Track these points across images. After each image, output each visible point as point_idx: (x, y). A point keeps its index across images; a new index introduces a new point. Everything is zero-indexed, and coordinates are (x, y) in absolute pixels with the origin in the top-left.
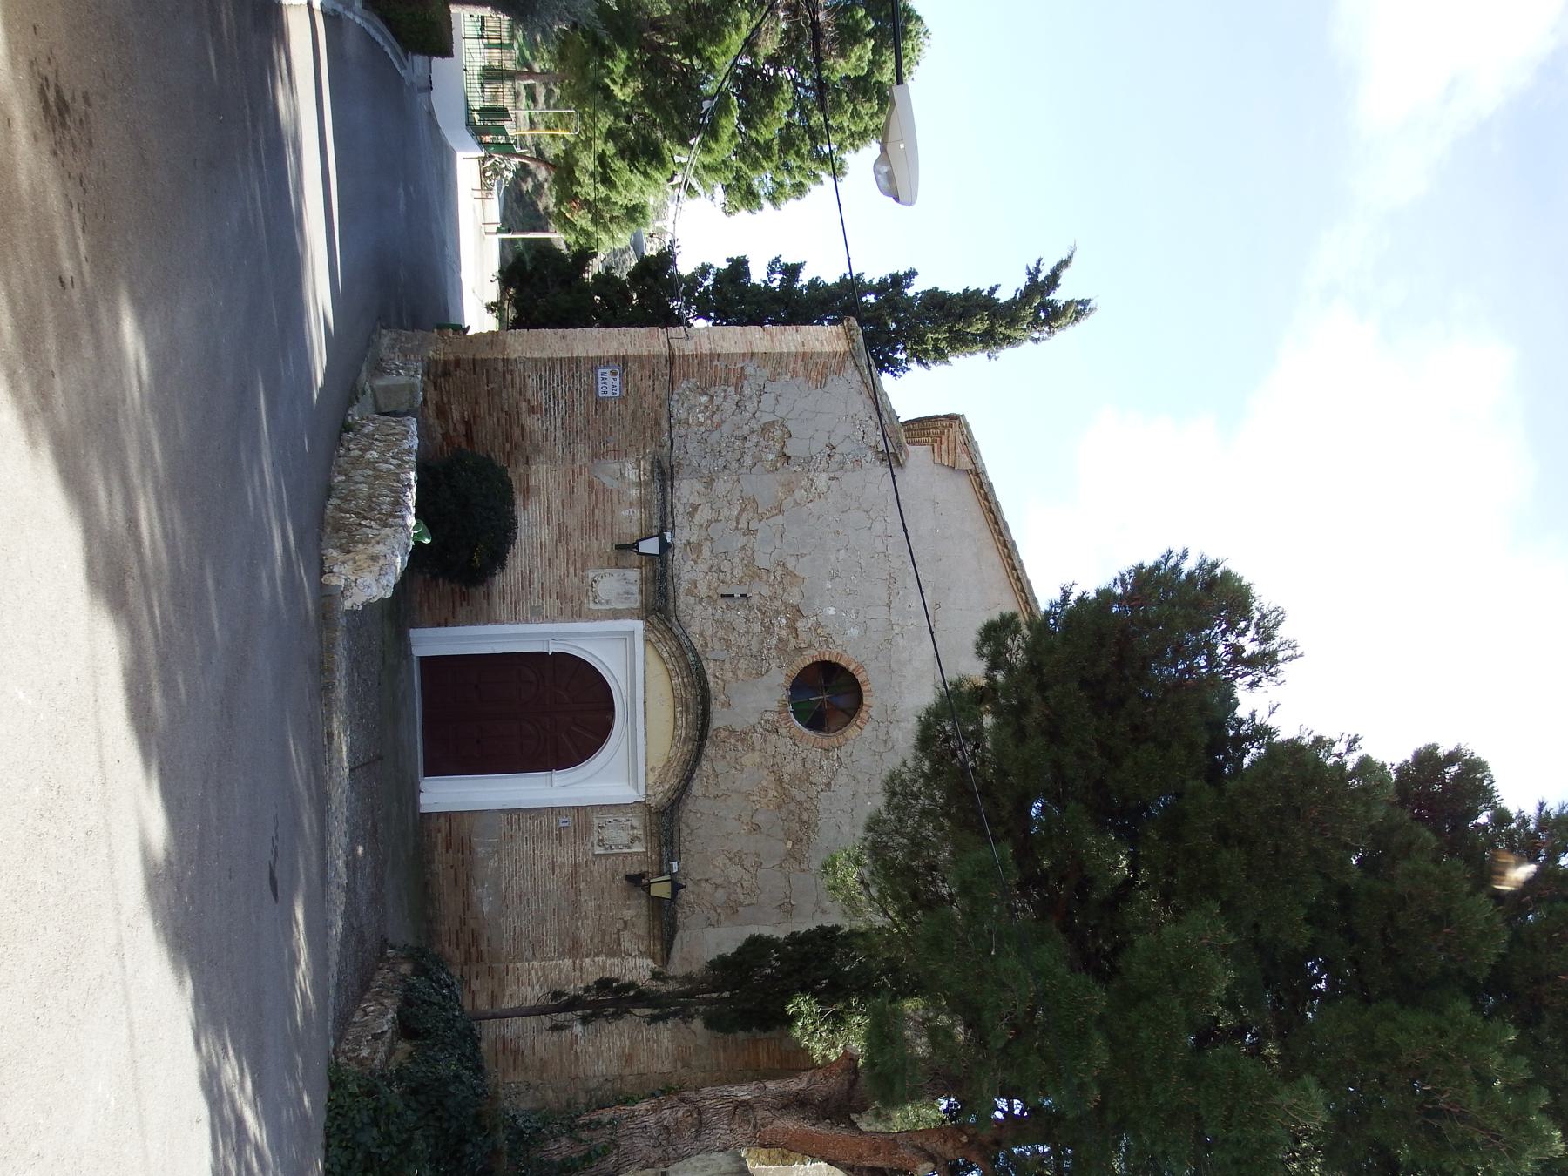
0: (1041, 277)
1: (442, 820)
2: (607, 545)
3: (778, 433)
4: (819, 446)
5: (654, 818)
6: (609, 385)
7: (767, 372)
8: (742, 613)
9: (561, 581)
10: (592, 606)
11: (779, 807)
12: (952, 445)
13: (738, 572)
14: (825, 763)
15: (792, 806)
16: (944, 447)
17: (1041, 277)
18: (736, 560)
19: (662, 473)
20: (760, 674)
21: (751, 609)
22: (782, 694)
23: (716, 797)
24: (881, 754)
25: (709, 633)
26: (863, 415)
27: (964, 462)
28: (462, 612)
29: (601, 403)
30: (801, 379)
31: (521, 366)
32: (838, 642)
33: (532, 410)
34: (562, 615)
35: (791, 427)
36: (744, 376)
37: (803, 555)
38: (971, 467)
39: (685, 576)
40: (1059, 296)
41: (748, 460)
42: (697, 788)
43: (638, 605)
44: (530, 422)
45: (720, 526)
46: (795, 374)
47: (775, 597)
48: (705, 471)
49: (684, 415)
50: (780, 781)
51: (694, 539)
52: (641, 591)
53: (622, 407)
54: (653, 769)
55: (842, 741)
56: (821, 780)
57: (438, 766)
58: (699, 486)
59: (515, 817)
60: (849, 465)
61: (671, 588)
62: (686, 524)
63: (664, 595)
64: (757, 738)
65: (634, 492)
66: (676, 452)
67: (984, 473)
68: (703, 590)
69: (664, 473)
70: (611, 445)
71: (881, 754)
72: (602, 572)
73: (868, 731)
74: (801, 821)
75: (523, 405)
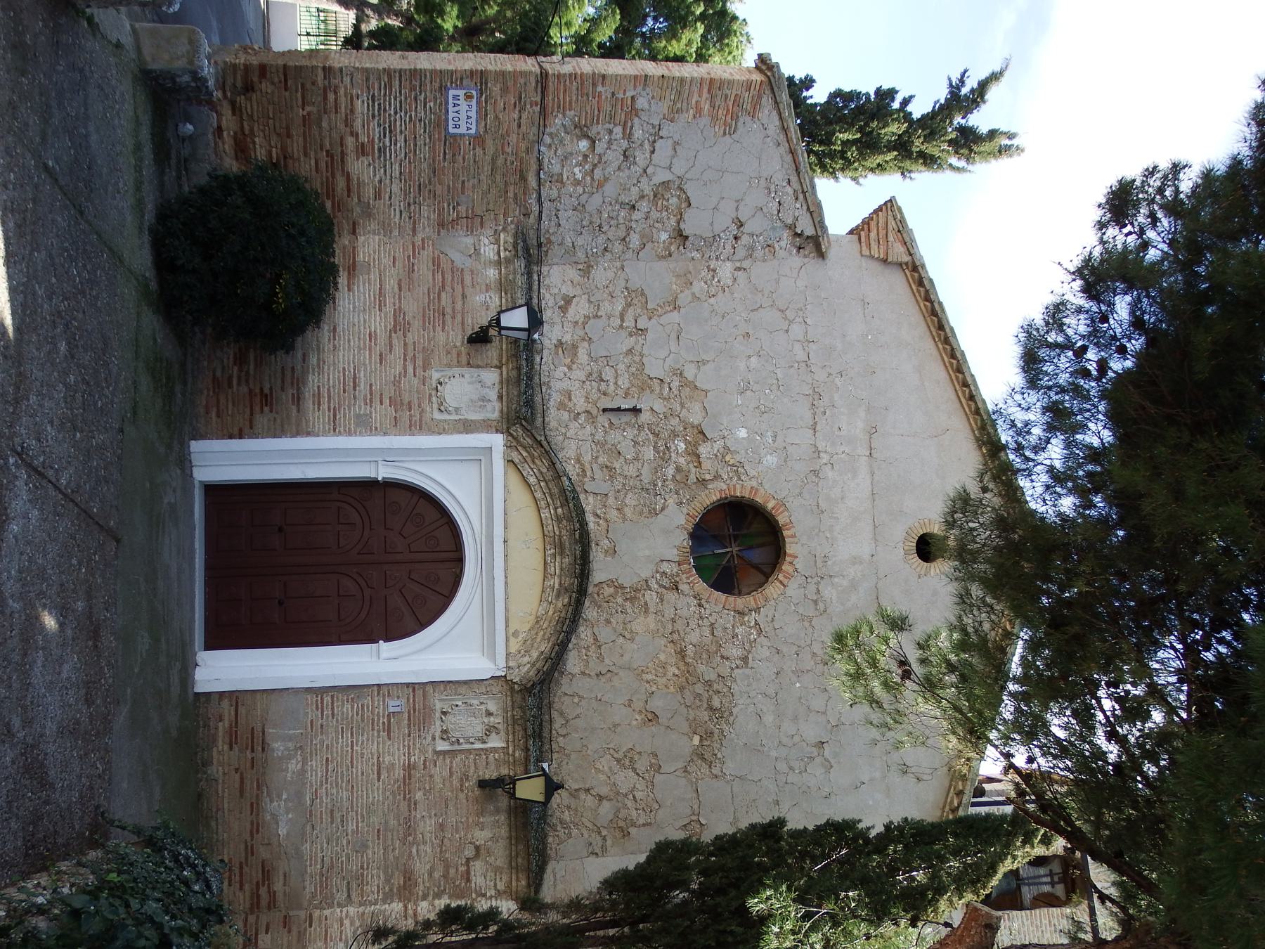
0: (964, 91)
1: (225, 703)
2: (456, 337)
3: (674, 201)
4: (723, 222)
5: (518, 698)
6: (463, 115)
7: (664, 107)
8: (630, 433)
9: (396, 383)
10: (437, 415)
11: (682, 689)
12: (882, 233)
13: (624, 382)
14: (740, 630)
15: (699, 688)
16: (873, 235)
17: (964, 91)
18: (621, 367)
19: (527, 249)
20: (654, 513)
21: (640, 428)
22: (683, 539)
23: (599, 675)
24: (810, 619)
25: (587, 458)
26: (779, 178)
27: (898, 252)
28: (261, 420)
29: (452, 142)
30: (705, 120)
31: (347, 80)
32: (752, 473)
33: (362, 150)
34: (397, 426)
35: (690, 189)
36: (634, 112)
37: (705, 362)
38: (906, 258)
39: (556, 385)
40: (980, 120)
41: (635, 240)
42: (573, 663)
43: (496, 415)
44: (360, 168)
45: (601, 323)
46: (698, 112)
47: (671, 414)
48: (581, 255)
49: (556, 168)
50: (682, 654)
51: (567, 338)
52: (500, 397)
53: (479, 151)
54: (516, 634)
55: (761, 602)
56: (736, 652)
57: (225, 635)
58: (572, 273)
59: (327, 699)
60: (759, 253)
61: (538, 399)
62: (557, 319)
63: (529, 403)
64: (651, 597)
65: (492, 273)
66: (545, 223)
67: (923, 266)
68: (580, 403)
69: (530, 251)
70: (462, 209)
71: (810, 619)
72: (449, 372)
73: (793, 589)
74: (711, 708)
75: (350, 141)
